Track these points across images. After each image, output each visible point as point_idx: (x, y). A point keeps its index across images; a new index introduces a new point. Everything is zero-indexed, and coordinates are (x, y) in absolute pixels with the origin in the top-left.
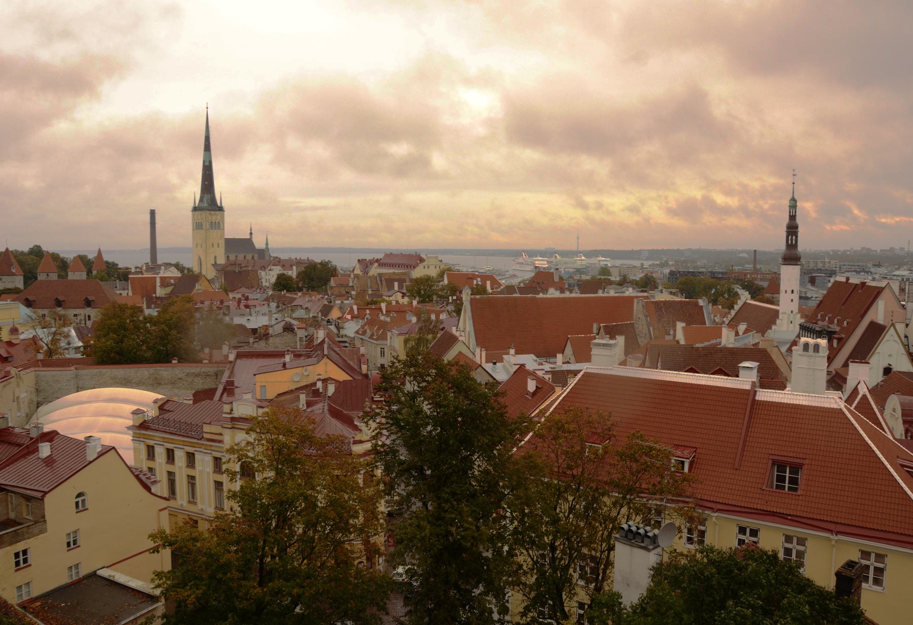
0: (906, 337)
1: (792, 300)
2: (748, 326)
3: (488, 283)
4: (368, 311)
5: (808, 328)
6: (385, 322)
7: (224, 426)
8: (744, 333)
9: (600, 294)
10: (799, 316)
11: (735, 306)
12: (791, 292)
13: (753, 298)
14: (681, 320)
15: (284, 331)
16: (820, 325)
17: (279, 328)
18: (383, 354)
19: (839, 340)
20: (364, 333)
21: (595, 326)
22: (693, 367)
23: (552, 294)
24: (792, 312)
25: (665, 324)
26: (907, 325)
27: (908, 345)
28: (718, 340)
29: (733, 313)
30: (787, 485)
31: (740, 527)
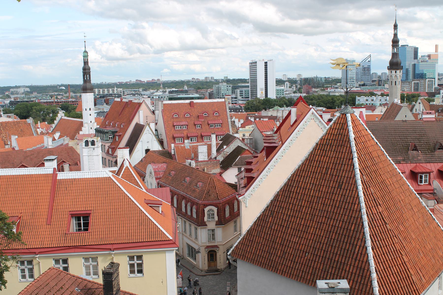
0: (156, 130)
1: (90, 115)
2: (61, 134)
5: (99, 130)
8: (59, 138)
10: (96, 124)
11: (55, 121)
12: (89, 109)
14: (15, 135)
19: (119, 136)
22: (24, 164)
24: (91, 122)
25: (4, 138)
26: (156, 124)
27: (158, 135)
28: (42, 145)
29: (54, 126)
30: (82, 228)
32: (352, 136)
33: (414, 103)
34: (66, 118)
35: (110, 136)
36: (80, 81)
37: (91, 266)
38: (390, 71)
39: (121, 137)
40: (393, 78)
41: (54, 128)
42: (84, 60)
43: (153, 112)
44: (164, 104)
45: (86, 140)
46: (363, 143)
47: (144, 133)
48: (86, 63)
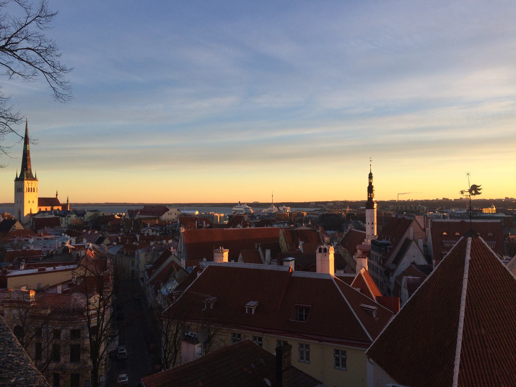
0: (425, 246)
1: (372, 228)
3: (204, 222)
4: (128, 240)
6: (136, 246)
7: (5, 306)
9: (269, 227)
12: (371, 224)
13: (355, 228)
14: (302, 241)
15: (63, 252)
16: (384, 241)
17: (60, 251)
18: (133, 265)
20: (123, 252)
21: (256, 244)
23: (239, 228)
24: (373, 235)
26: (427, 240)
31: (278, 341)
32: (468, 257)
34: (355, 230)
35: (382, 248)
36: (366, 199)
37: (305, 352)
39: (392, 250)
41: (344, 237)
42: (369, 180)
43: (424, 230)
44: (434, 222)
45: (320, 247)
46: (481, 266)
47: (411, 247)
48: (370, 184)
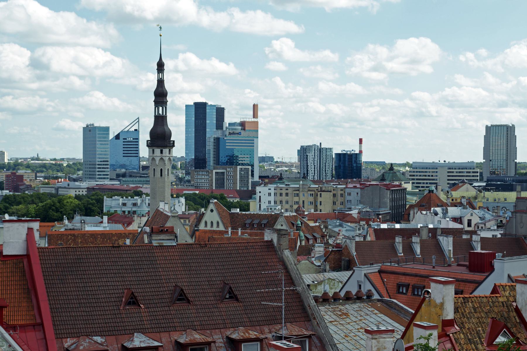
33: (203, 210)
38: (151, 150)
40: (157, 162)
